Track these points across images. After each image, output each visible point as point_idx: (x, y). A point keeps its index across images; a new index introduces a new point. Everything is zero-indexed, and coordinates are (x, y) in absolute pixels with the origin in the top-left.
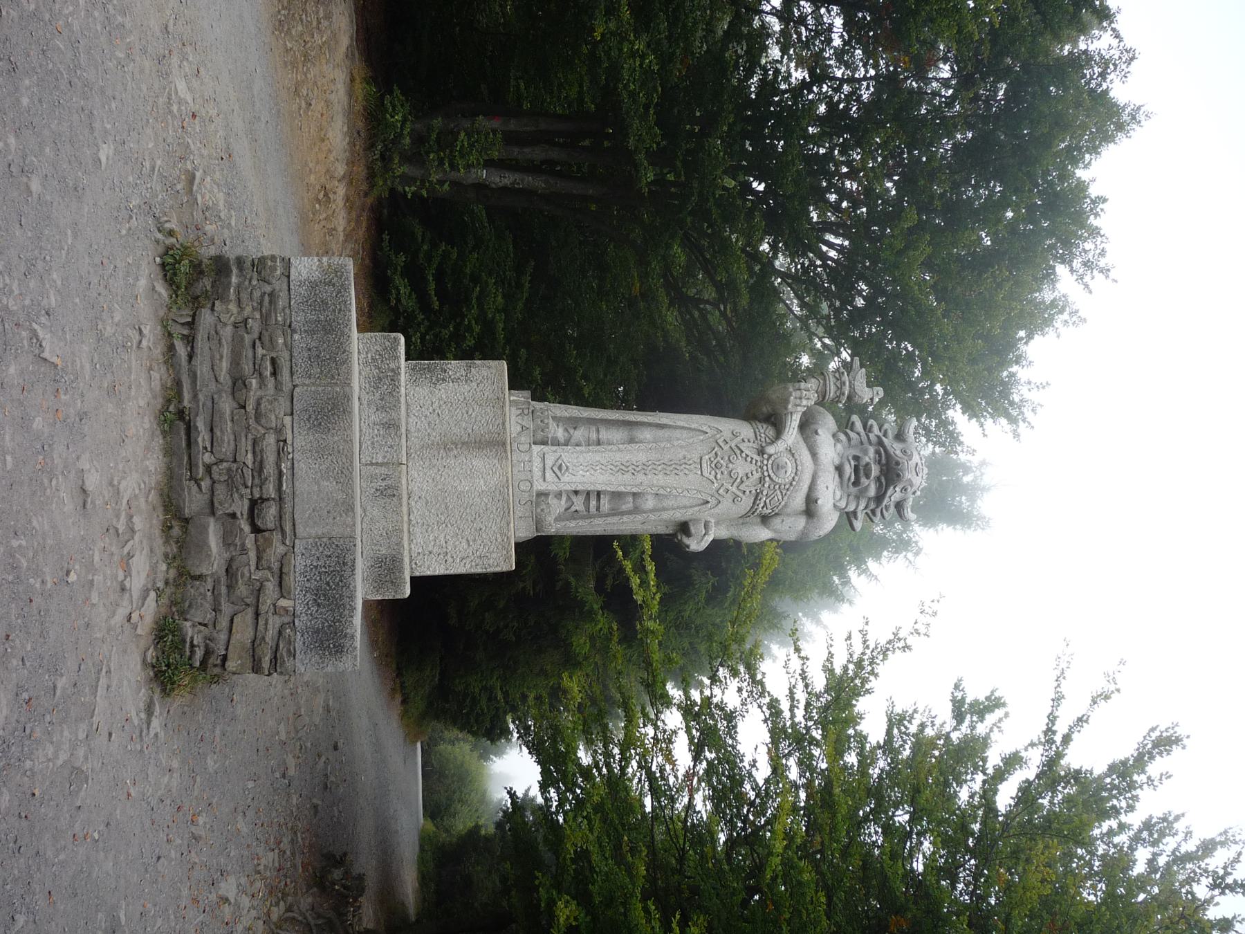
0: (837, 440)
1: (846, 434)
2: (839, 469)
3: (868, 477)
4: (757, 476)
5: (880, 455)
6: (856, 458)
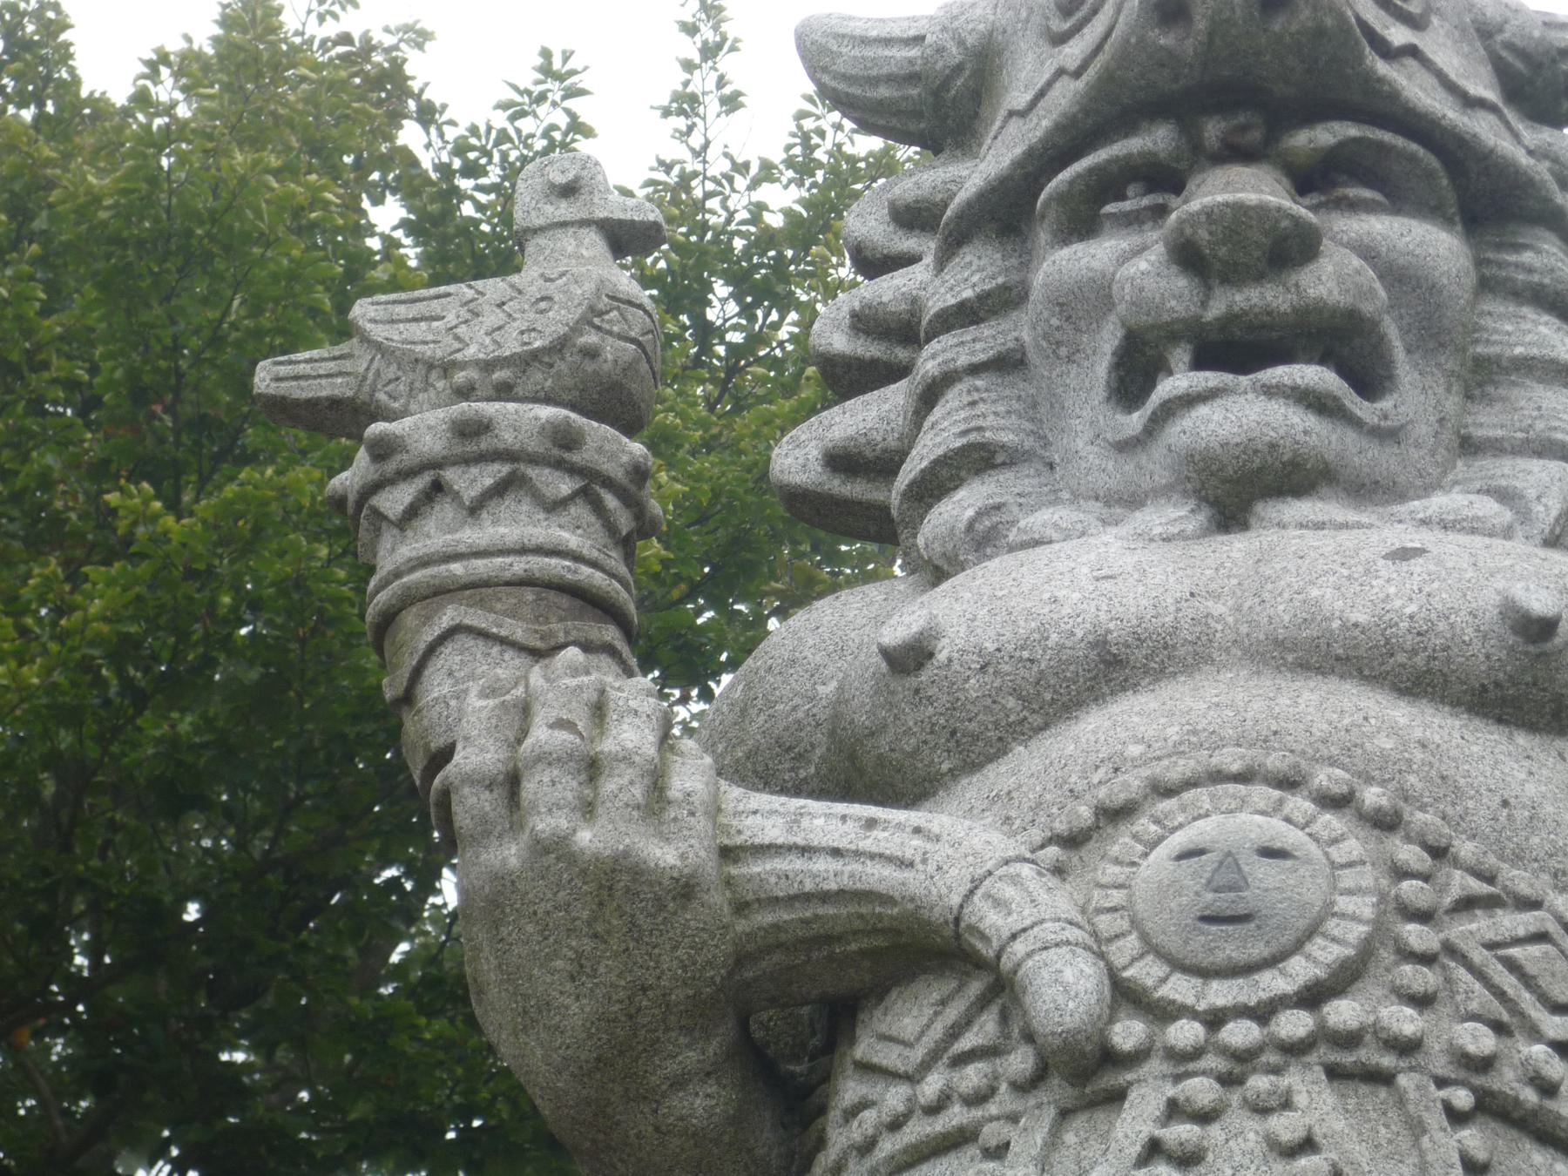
0: (984, 539)
1: (932, 487)
2: (1234, 493)
3: (1290, 249)
4: (1314, 1101)
5: (1108, 185)
6: (1134, 373)
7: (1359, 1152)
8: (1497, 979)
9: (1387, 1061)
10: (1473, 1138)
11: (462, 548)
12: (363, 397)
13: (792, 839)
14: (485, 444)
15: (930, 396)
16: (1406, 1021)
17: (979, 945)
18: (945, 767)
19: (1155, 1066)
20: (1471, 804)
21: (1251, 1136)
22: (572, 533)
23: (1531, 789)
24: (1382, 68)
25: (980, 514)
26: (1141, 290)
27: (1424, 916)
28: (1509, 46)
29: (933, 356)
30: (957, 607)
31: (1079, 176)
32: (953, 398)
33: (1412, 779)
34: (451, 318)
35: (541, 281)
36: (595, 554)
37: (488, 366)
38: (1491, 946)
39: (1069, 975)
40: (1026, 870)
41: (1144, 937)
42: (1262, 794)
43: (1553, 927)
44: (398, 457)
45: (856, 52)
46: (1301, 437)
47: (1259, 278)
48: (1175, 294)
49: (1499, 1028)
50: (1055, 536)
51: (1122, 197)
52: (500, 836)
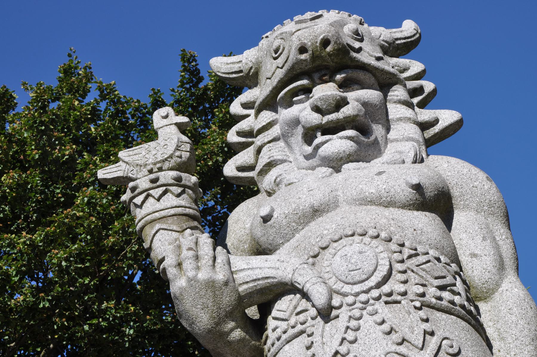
1: (264, 172)
2: (336, 164)
3: (342, 103)
7: (396, 321)
8: (420, 274)
9: (399, 298)
10: (422, 314)
11: (158, 209)
12: (125, 175)
13: (249, 267)
15: (259, 151)
16: (402, 288)
17: (298, 286)
18: (281, 242)
19: (344, 308)
20: (407, 232)
21: (370, 321)
22: (184, 201)
23: (420, 225)
24: (354, 55)
25: (276, 178)
27: (402, 261)
28: (383, 41)
29: (259, 140)
30: (277, 203)
32: (265, 150)
33: (392, 228)
34: (144, 153)
35: (164, 141)
36: (189, 205)
37: (155, 164)
38: (417, 266)
39: (320, 290)
40: (306, 266)
41: (336, 277)
42: (357, 238)
43: (432, 259)
44: (138, 190)
45: (226, 67)
46: (350, 148)
47: (334, 112)
48: (315, 119)
49: (424, 285)
50: (296, 181)
51: (297, 96)
52: (180, 278)
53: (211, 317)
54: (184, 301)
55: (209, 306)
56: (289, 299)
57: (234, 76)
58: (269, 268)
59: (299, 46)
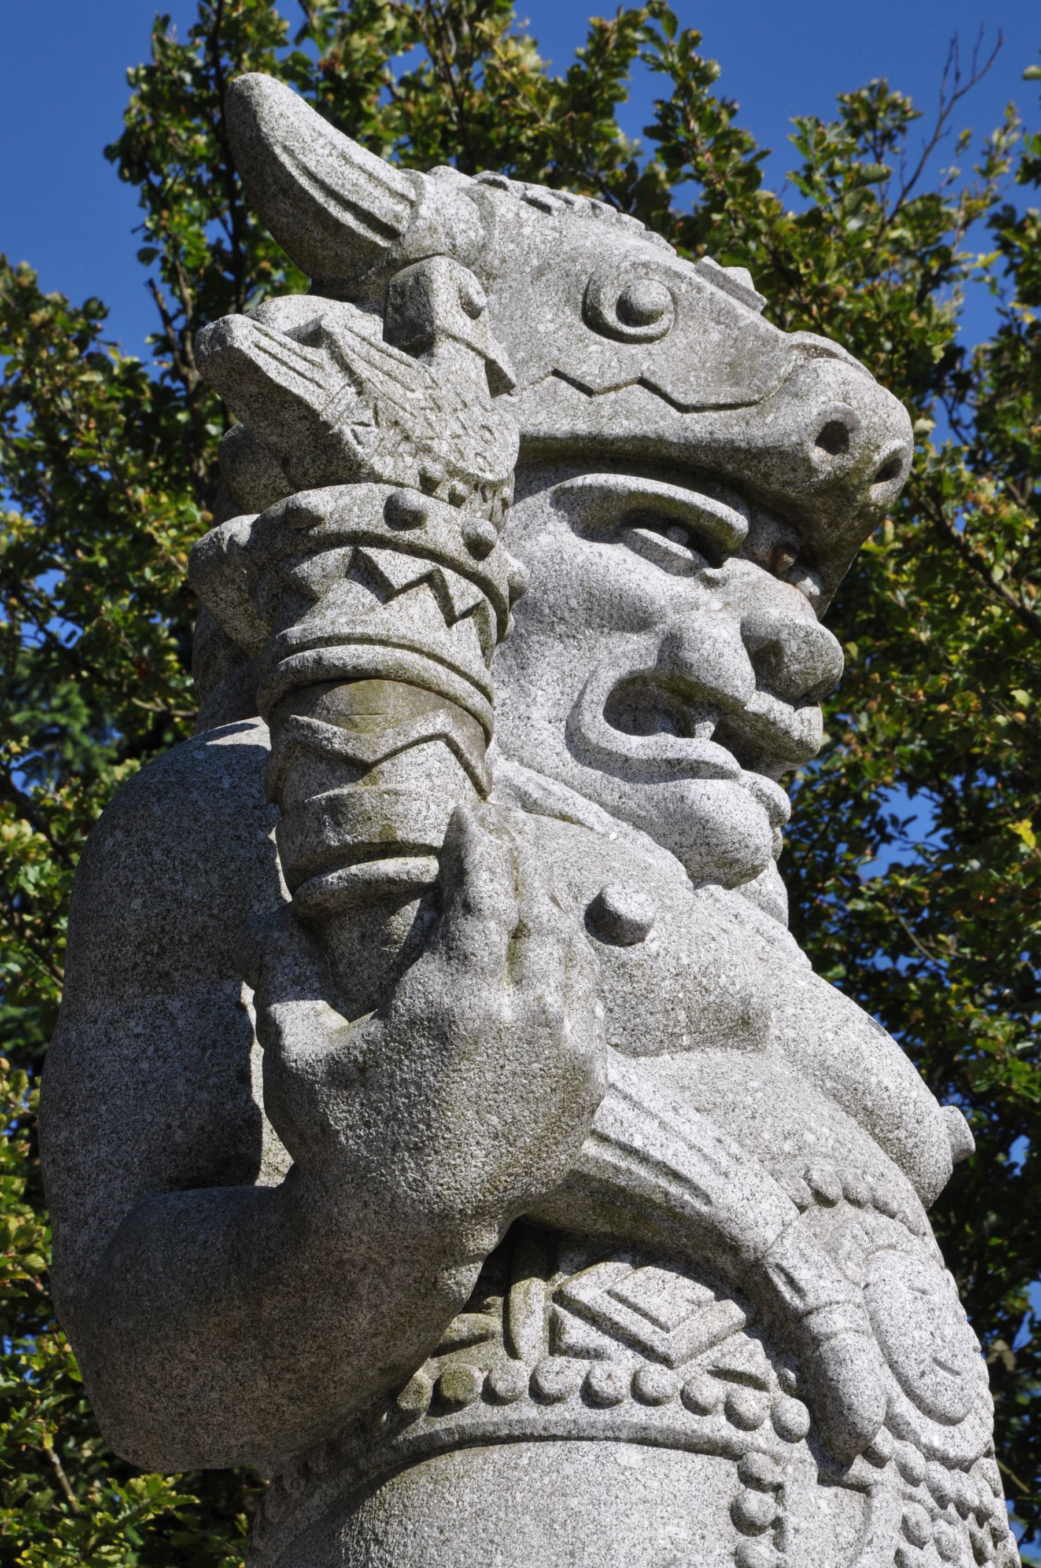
14: (481, 567)
26: (721, 655)
31: (643, 494)
37: (453, 472)
44: (417, 532)
53: (492, 1178)
54: (464, 1065)
55: (519, 1144)
56: (689, 1294)
57: (348, 219)
58: (691, 1147)
59: (835, 417)
